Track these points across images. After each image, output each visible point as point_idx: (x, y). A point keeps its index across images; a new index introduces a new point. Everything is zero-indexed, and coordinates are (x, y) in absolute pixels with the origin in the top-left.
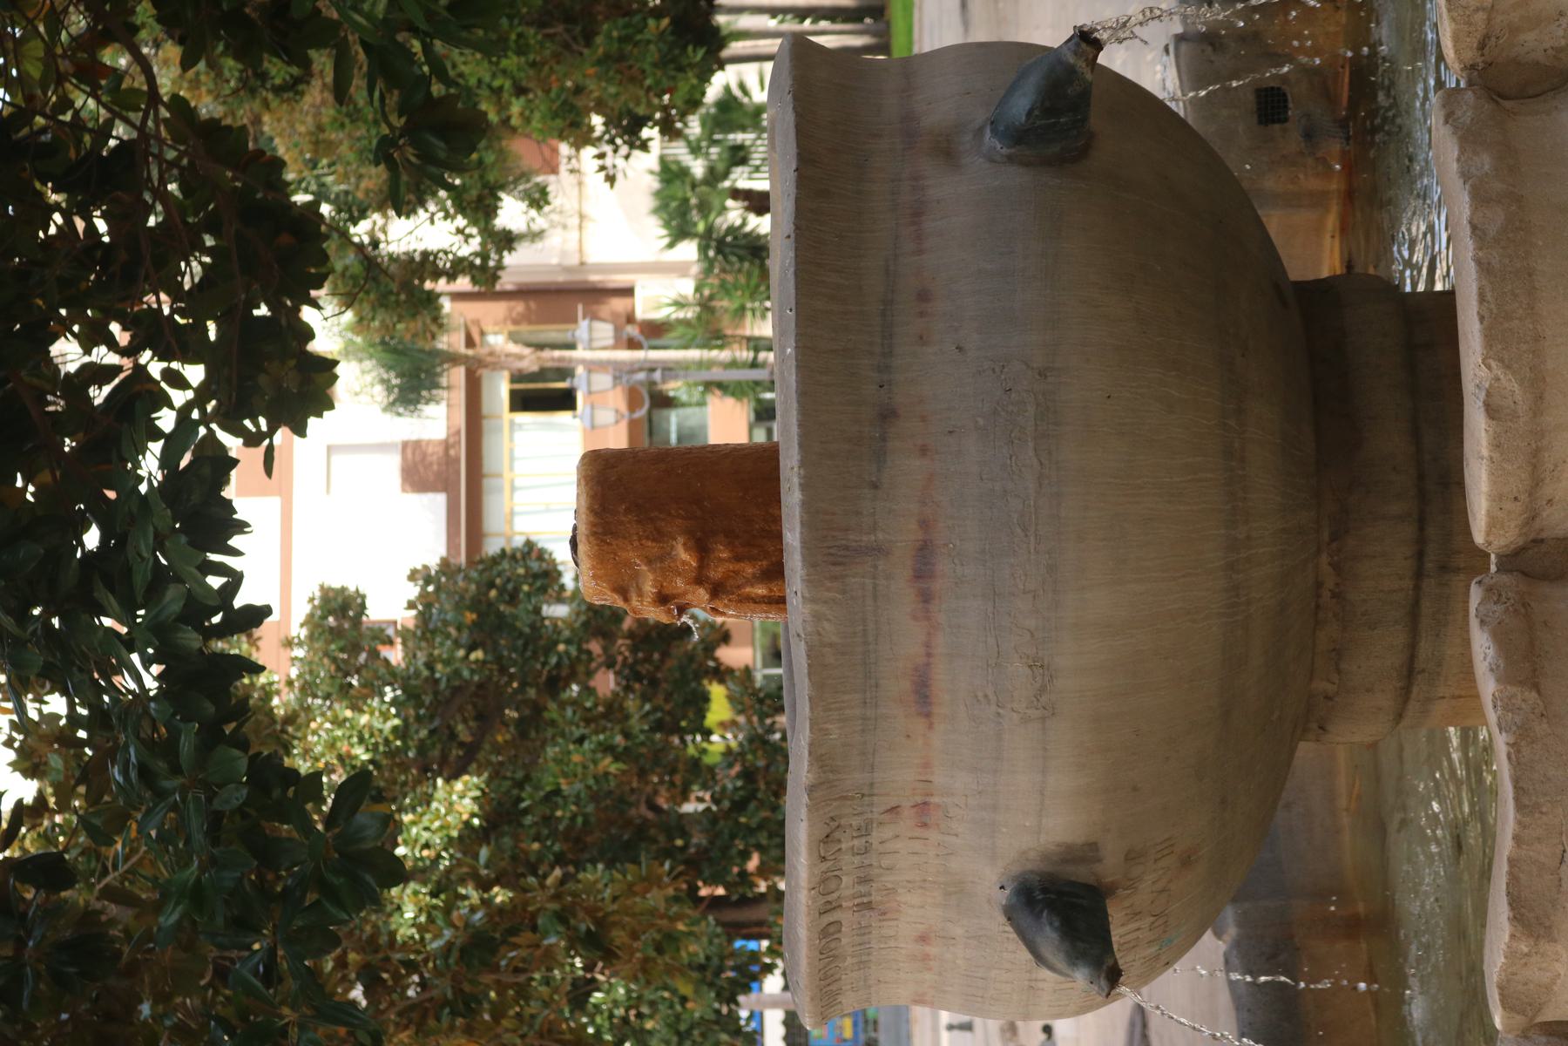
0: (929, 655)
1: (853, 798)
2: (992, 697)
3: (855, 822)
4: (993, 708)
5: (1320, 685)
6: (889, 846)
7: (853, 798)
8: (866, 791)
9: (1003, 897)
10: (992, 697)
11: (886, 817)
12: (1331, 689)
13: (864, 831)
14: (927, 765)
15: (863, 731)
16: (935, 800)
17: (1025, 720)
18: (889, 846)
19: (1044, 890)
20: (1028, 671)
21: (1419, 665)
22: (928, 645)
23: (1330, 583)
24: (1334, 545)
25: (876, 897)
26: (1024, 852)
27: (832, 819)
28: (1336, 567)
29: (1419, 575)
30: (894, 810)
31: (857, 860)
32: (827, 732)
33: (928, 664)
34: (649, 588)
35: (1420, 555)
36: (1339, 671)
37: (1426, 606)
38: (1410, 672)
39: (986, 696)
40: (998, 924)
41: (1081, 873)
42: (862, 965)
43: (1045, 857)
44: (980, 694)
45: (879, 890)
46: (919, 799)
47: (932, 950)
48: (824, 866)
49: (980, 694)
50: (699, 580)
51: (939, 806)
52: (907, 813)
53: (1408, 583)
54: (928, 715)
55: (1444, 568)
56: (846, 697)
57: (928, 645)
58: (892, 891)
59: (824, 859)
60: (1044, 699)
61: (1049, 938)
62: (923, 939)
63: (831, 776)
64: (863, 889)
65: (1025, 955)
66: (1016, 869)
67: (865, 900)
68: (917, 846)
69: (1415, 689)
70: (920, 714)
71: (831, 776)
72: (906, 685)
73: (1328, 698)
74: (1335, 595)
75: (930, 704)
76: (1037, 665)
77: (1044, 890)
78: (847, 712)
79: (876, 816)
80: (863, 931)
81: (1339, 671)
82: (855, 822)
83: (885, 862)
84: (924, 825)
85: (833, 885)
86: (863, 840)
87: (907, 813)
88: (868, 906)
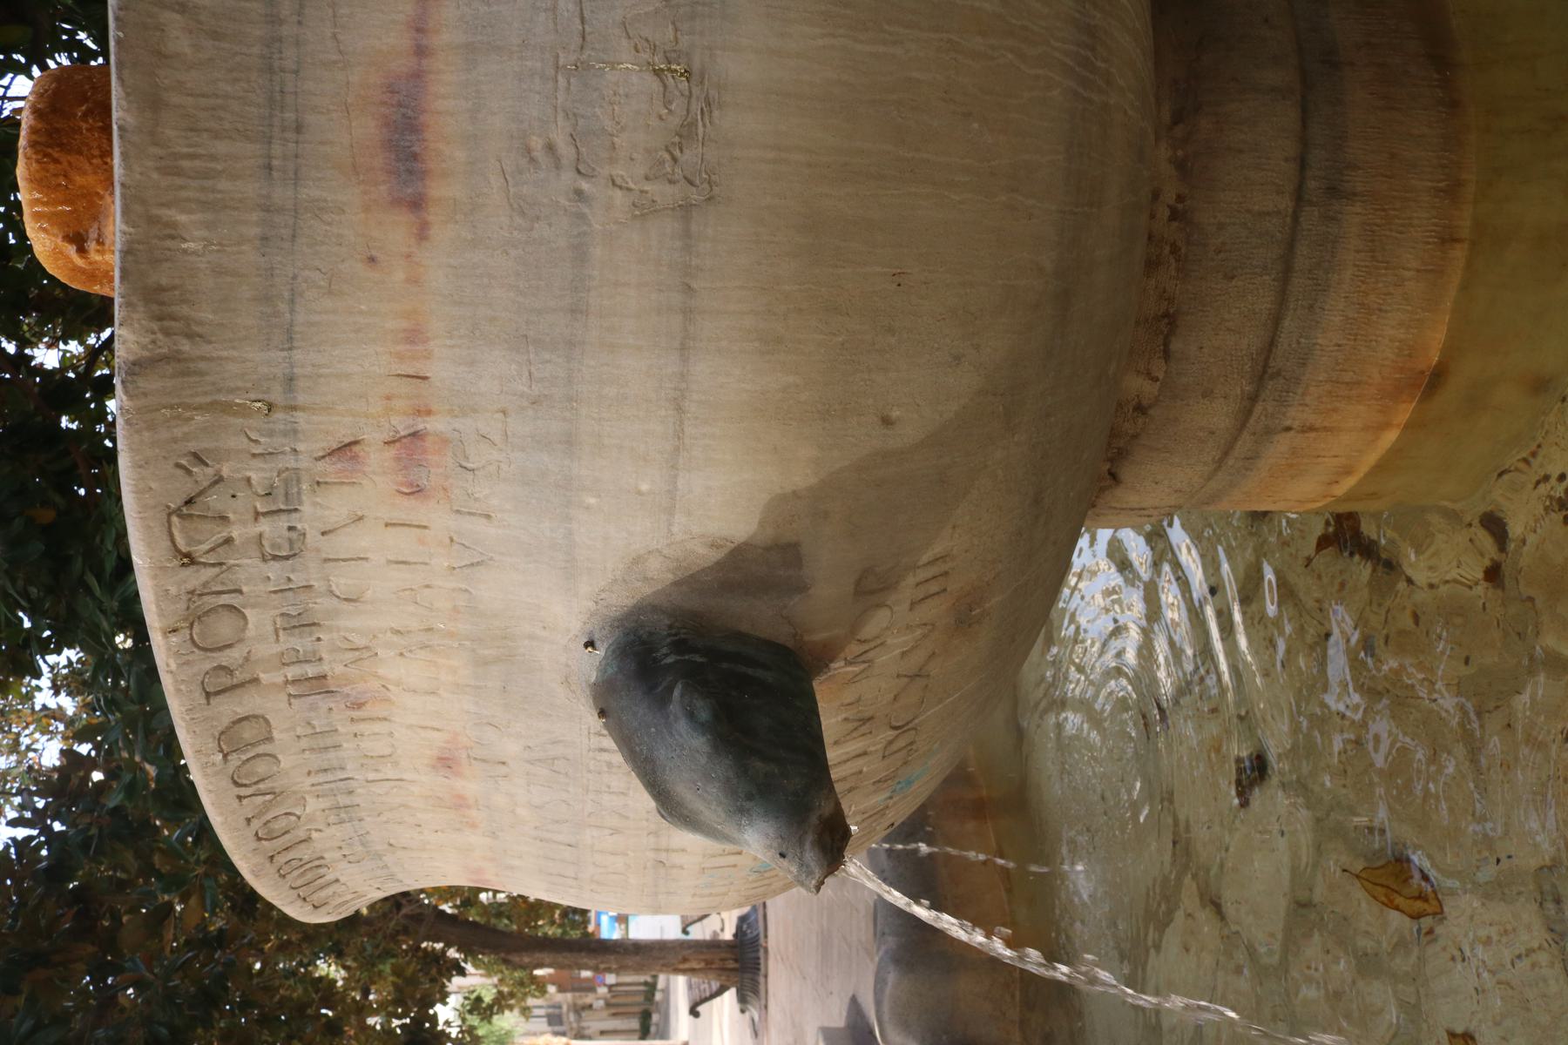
0: (421, 51)
1: (243, 411)
2: (565, 150)
3: (259, 474)
4: (568, 177)
5: (1136, 385)
6: (342, 544)
8: (277, 395)
9: (589, 665)
10: (565, 150)
11: (328, 468)
12: (1149, 389)
13: (281, 500)
14: (414, 336)
15: (264, 239)
16: (436, 425)
17: (644, 211)
18: (342, 544)
19: (680, 646)
20: (653, 84)
22: (419, 28)
23: (1169, 196)
24: (1179, 131)
25: (333, 666)
26: (637, 560)
27: (198, 458)
28: (1181, 166)
29: (1299, 197)
30: (346, 450)
31: (274, 570)
32: (173, 232)
33: (417, 75)
35: (1303, 164)
36: (1167, 355)
38: (1263, 373)
39: (550, 148)
40: (585, 733)
41: (758, 616)
42: (344, 812)
43: (691, 582)
44: (537, 143)
45: (335, 650)
46: (402, 425)
47: (470, 786)
48: (196, 578)
49: (537, 143)
51: (445, 441)
52: (377, 458)
53: (1286, 203)
54: (417, 204)
55: (1334, 191)
56: (222, 147)
57: (419, 28)
58: (362, 653)
59: (189, 560)
60: (688, 156)
61: (687, 746)
62: (446, 763)
63: (186, 346)
64: (302, 643)
65: (644, 801)
66: (622, 600)
67: (311, 670)
68: (402, 543)
70: (396, 202)
71: (186, 346)
72: (366, 128)
73: (1140, 409)
74: (1174, 215)
75: (423, 175)
76: (675, 69)
77: (680, 646)
78: (224, 184)
79: (304, 463)
80: (322, 741)
82: (259, 474)
83: (343, 581)
84: (417, 491)
85: (223, 627)
86: (283, 522)
87: (377, 458)
88: (319, 685)
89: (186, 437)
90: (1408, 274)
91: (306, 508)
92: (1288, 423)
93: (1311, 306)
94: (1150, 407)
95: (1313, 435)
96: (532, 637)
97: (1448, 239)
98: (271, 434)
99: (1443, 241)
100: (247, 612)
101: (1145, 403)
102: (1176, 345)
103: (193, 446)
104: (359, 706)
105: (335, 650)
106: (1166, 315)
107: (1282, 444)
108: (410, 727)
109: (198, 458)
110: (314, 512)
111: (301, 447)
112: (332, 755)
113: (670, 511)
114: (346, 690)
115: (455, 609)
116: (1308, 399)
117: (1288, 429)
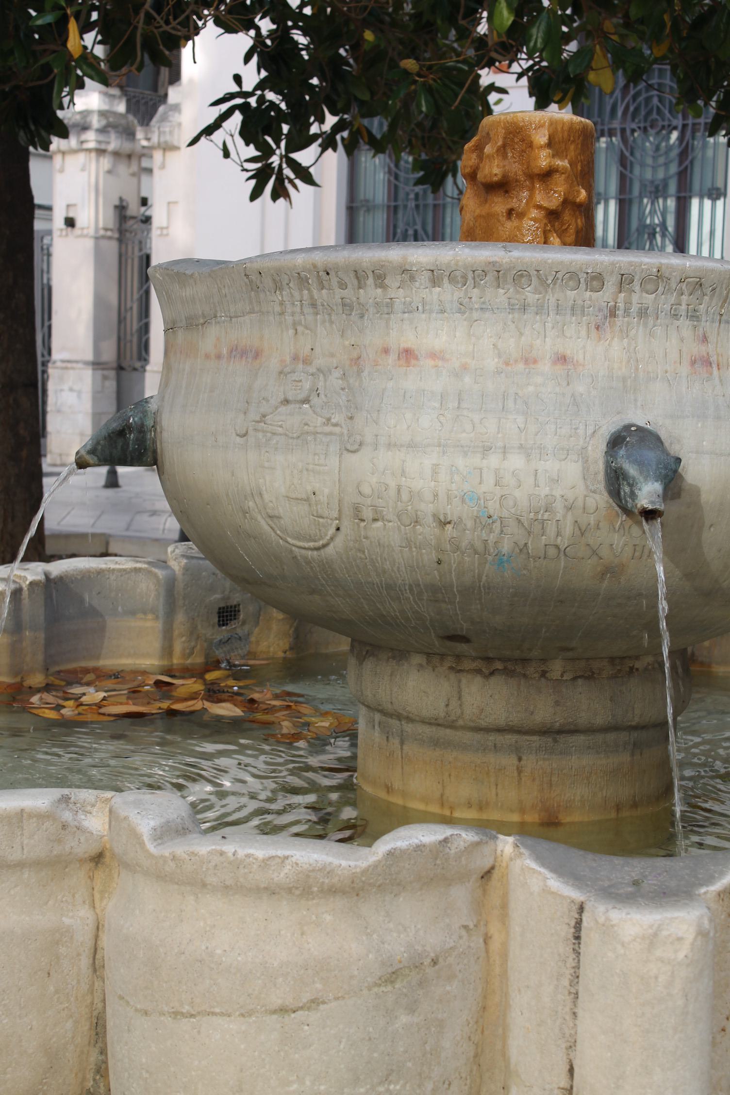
1: (722, 307)
7: (722, 307)
8: (724, 318)
13: (694, 316)
21: (562, 738)
25: (619, 321)
29: (635, 728)
30: (705, 339)
31: (667, 307)
34: (562, 163)
36: (575, 679)
37: (611, 737)
45: (628, 324)
46: (713, 359)
50: (565, 202)
51: (711, 374)
52: (703, 349)
53: (636, 721)
67: (620, 313)
69: (535, 738)
73: (544, 674)
74: (631, 668)
79: (703, 324)
81: (575, 679)
83: (658, 330)
84: (693, 363)
86: (684, 313)
89: (722, 288)
90: (604, 791)
91: (688, 322)
92: (524, 758)
93: (589, 747)
94: (547, 678)
95: (516, 774)
96: (636, 400)
97: (618, 808)
98: (714, 314)
99: (618, 806)
100: (654, 295)
101: (548, 675)
102: (580, 682)
103: (718, 290)
104: (598, 328)
105: (628, 324)
106: (593, 673)
107: (510, 761)
108: (584, 347)
109: (714, 289)
110: (685, 324)
111: (708, 323)
112: (579, 312)
113: (697, 452)
114: (607, 324)
115: (648, 372)
116: (540, 763)
117: (520, 759)
